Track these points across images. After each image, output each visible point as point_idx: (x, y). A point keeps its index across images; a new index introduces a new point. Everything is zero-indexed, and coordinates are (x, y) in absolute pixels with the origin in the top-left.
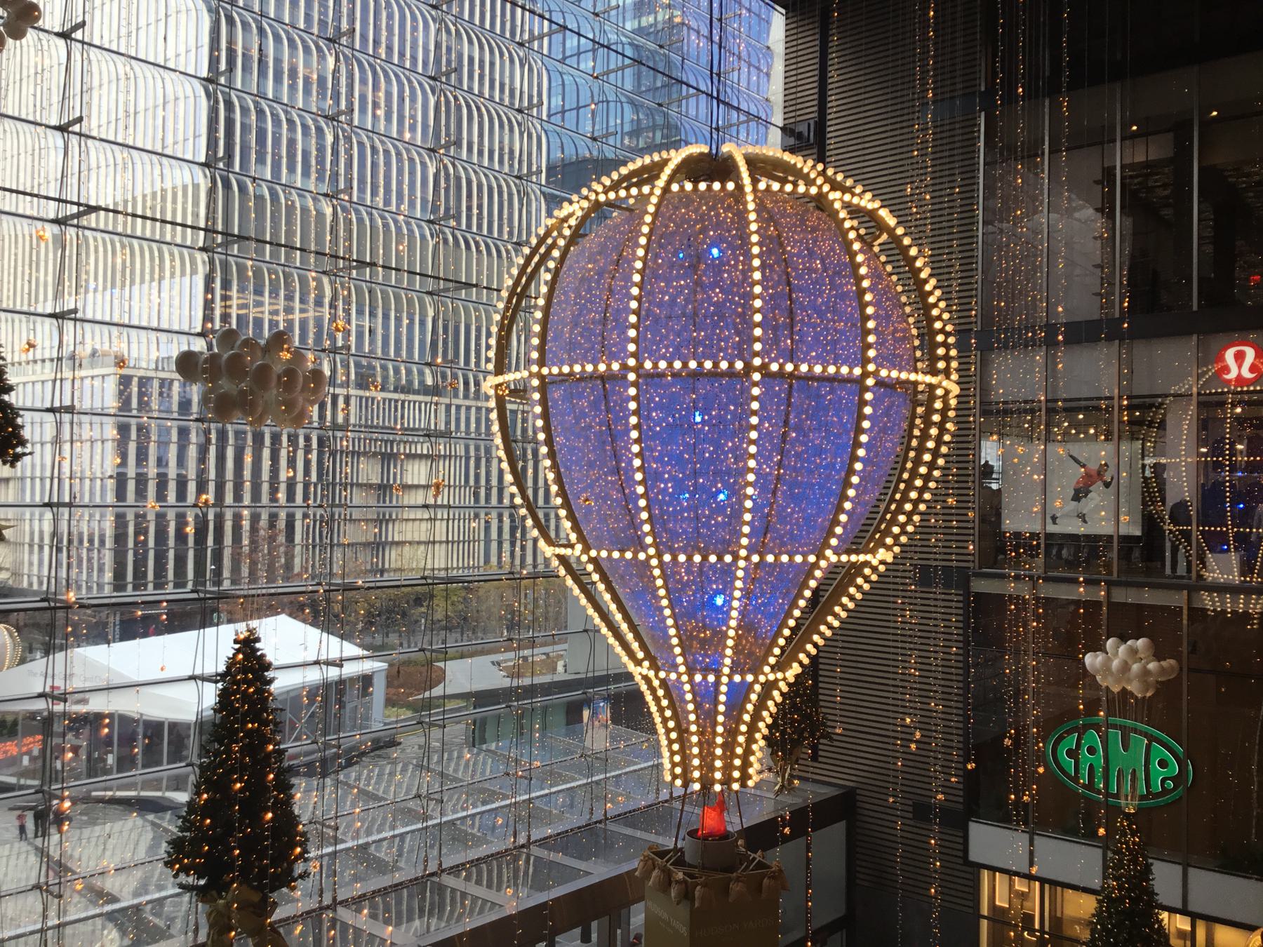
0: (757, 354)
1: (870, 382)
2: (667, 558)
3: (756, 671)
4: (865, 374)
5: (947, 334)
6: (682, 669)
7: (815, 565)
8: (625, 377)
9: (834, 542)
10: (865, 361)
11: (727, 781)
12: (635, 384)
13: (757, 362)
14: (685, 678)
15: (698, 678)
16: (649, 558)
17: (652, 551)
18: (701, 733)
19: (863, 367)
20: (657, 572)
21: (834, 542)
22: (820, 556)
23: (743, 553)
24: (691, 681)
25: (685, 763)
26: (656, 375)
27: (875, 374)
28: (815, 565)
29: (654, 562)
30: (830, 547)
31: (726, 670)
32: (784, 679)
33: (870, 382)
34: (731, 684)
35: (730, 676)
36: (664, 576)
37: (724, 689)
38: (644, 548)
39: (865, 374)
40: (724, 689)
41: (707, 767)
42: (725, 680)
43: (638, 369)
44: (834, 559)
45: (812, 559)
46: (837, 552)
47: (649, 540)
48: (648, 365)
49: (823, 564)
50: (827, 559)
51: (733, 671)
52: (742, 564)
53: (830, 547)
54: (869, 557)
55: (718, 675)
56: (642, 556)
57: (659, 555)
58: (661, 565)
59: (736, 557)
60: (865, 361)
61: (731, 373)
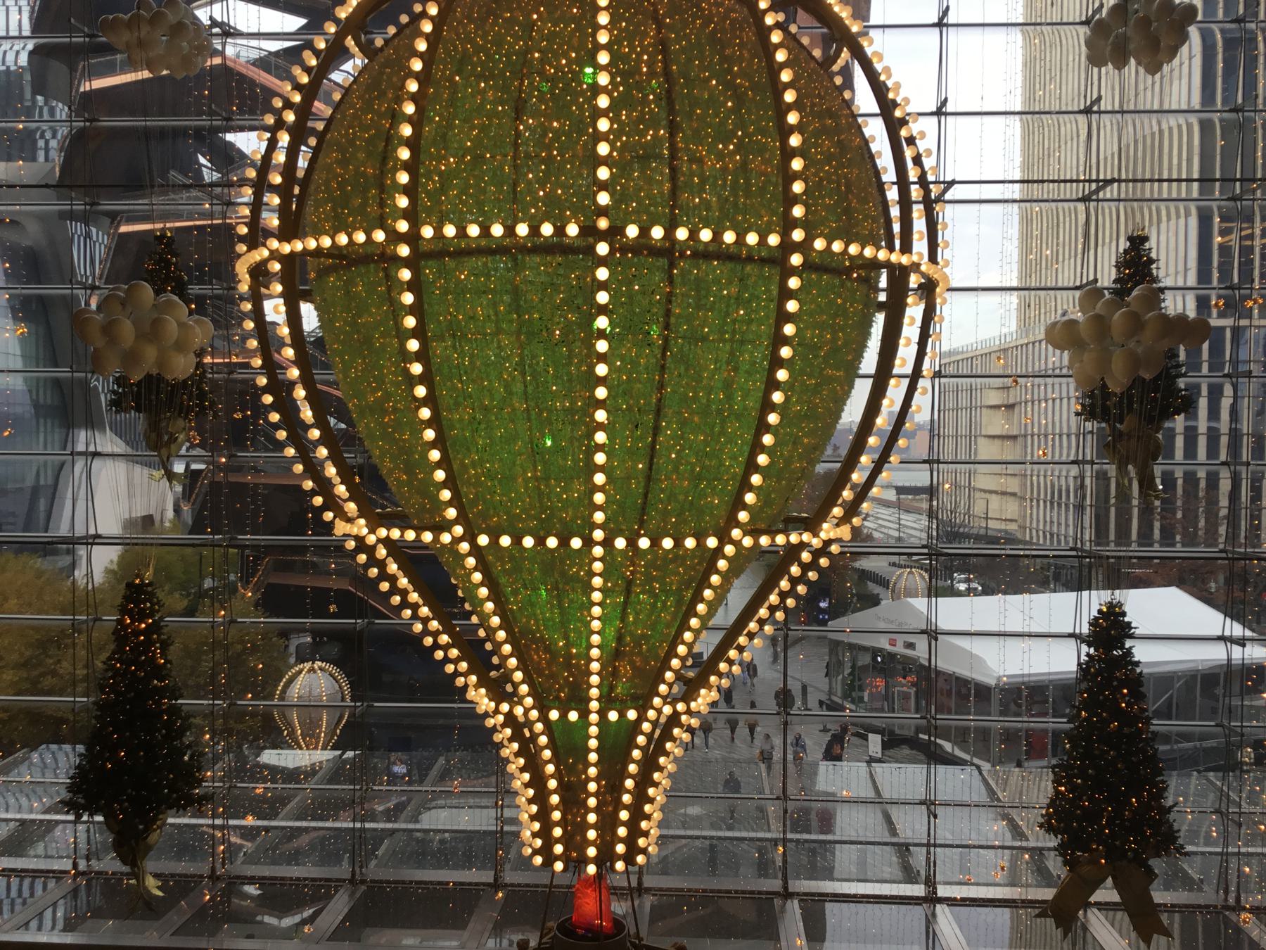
0: (603, 211)
1: (796, 260)
2: (483, 540)
3: (643, 706)
4: (788, 247)
5: (278, 113)
6: (529, 701)
7: (718, 552)
8: (591, 250)
9: (743, 516)
10: (788, 224)
11: (606, 858)
12: (407, 263)
13: (603, 224)
14: (534, 714)
15: (554, 715)
16: (456, 541)
17: (458, 530)
18: (563, 789)
19: (785, 235)
20: (471, 562)
21: (743, 516)
22: (724, 538)
23: (598, 535)
24: (544, 718)
25: (545, 833)
26: (441, 251)
27: (804, 247)
28: (718, 552)
29: (464, 547)
30: (738, 524)
31: (594, 705)
32: (689, 712)
33: (796, 260)
34: (603, 722)
35: (602, 713)
36: (482, 566)
37: (594, 730)
38: (446, 526)
39: (788, 247)
40: (594, 730)
41: (574, 839)
42: (594, 718)
43: (413, 238)
44: (748, 542)
45: (712, 542)
46: (754, 532)
47: (451, 513)
48: (427, 232)
49: (729, 550)
50: (737, 544)
51: (608, 701)
52: (598, 551)
53: (738, 524)
54: (806, 537)
55: (585, 713)
56: (446, 538)
57: (470, 536)
58: (476, 550)
59: (589, 542)
60: (788, 224)
61: (558, 246)
